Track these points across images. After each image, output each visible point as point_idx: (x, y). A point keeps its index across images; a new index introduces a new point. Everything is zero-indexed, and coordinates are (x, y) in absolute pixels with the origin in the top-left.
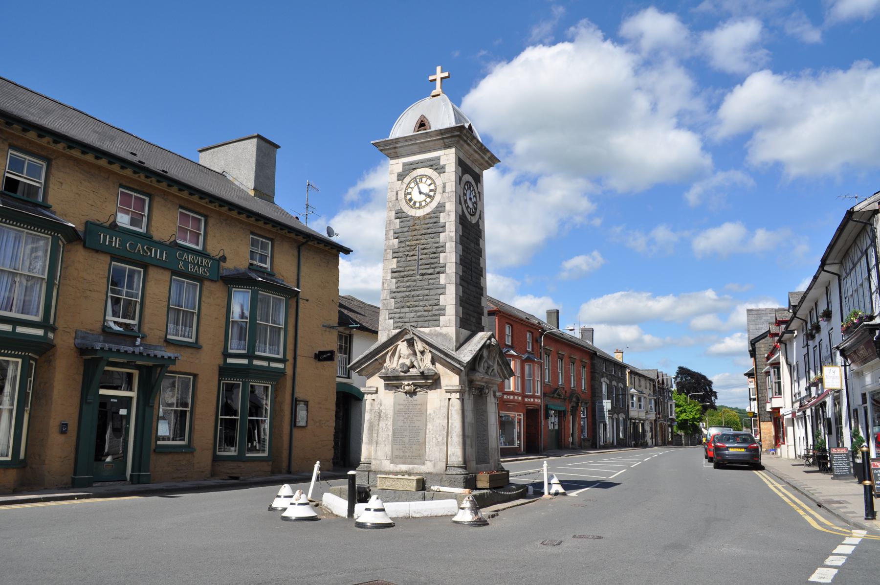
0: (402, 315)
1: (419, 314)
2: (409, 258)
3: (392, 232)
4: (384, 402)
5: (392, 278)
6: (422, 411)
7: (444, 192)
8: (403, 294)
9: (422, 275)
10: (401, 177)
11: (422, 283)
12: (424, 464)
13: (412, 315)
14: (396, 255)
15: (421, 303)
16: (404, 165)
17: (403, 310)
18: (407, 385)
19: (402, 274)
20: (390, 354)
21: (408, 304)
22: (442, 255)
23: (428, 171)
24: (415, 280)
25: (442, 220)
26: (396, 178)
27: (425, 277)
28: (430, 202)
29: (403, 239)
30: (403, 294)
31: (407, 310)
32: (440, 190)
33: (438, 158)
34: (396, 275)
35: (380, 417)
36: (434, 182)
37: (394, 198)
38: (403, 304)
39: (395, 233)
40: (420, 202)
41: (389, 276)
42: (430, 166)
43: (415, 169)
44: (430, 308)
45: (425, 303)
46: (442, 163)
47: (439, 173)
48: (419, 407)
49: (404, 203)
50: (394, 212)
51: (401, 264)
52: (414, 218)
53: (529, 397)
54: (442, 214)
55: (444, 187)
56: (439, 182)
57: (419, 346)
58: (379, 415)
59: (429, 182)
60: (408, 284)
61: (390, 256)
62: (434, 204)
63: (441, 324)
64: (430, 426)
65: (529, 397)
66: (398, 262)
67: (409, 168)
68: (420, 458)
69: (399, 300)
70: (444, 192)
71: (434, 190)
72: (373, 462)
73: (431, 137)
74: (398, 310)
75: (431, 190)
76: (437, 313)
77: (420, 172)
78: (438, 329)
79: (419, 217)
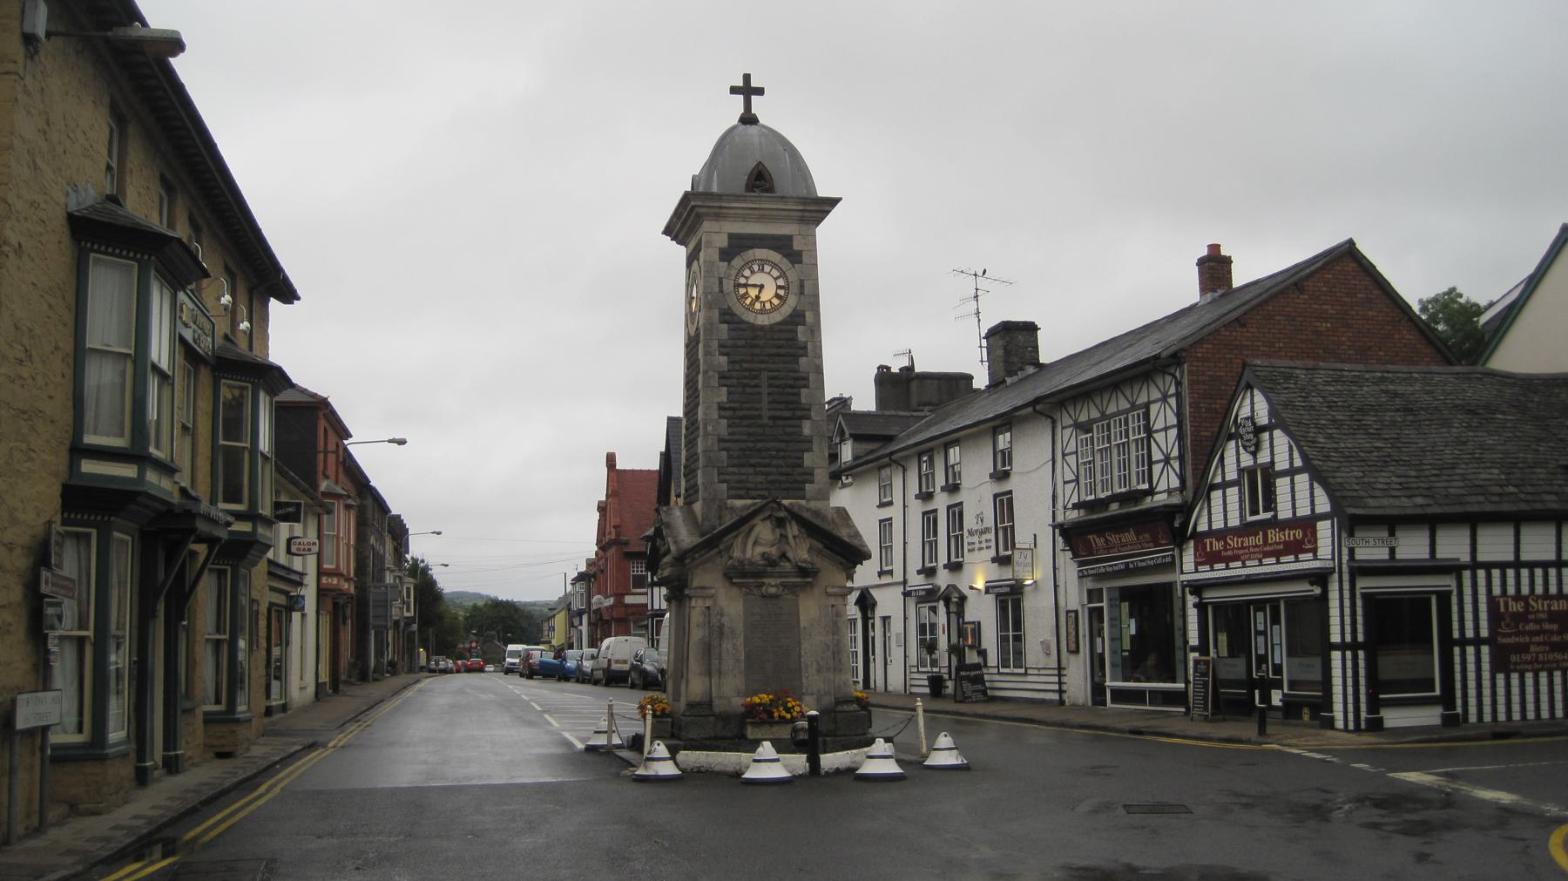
2: (749, 390)
3: (715, 344)
5: (721, 417)
7: (802, 293)
8: (743, 445)
10: (727, 255)
13: (760, 478)
16: (731, 236)
17: (743, 470)
18: (772, 585)
19: (740, 413)
21: (752, 461)
22: (804, 391)
23: (775, 256)
26: (716, 257)
27: (779, 422)
28: (780, 306)
29: (738, 358)
31: (751, 470)
32: (794, 288)
33: (789, 238)
34: (728, 413)
35: (721, 634)
37: (716, 289)
39: (721, 346)
42: (776, 249)
43: (751, 248)
44: (789, 470)
46: (796, 247)
47: (793, 263)
50: (717, 312)
52: (753, 327)
53: (330, 574)
54: (800, 328)
55: (802, 286)
58: (720, 631)
59: (775, 273)
60: (751, 430)
61: (715, 382)
62: (786, 310)
63: (808, 495)
64: (805, 645)
65: (330, 574)
66: (729, 393)
67: (737, 246)
69: (736, 454)
70: (802, 293)
72: (716, 702)
77: (761, 253)
78: (803, 502)
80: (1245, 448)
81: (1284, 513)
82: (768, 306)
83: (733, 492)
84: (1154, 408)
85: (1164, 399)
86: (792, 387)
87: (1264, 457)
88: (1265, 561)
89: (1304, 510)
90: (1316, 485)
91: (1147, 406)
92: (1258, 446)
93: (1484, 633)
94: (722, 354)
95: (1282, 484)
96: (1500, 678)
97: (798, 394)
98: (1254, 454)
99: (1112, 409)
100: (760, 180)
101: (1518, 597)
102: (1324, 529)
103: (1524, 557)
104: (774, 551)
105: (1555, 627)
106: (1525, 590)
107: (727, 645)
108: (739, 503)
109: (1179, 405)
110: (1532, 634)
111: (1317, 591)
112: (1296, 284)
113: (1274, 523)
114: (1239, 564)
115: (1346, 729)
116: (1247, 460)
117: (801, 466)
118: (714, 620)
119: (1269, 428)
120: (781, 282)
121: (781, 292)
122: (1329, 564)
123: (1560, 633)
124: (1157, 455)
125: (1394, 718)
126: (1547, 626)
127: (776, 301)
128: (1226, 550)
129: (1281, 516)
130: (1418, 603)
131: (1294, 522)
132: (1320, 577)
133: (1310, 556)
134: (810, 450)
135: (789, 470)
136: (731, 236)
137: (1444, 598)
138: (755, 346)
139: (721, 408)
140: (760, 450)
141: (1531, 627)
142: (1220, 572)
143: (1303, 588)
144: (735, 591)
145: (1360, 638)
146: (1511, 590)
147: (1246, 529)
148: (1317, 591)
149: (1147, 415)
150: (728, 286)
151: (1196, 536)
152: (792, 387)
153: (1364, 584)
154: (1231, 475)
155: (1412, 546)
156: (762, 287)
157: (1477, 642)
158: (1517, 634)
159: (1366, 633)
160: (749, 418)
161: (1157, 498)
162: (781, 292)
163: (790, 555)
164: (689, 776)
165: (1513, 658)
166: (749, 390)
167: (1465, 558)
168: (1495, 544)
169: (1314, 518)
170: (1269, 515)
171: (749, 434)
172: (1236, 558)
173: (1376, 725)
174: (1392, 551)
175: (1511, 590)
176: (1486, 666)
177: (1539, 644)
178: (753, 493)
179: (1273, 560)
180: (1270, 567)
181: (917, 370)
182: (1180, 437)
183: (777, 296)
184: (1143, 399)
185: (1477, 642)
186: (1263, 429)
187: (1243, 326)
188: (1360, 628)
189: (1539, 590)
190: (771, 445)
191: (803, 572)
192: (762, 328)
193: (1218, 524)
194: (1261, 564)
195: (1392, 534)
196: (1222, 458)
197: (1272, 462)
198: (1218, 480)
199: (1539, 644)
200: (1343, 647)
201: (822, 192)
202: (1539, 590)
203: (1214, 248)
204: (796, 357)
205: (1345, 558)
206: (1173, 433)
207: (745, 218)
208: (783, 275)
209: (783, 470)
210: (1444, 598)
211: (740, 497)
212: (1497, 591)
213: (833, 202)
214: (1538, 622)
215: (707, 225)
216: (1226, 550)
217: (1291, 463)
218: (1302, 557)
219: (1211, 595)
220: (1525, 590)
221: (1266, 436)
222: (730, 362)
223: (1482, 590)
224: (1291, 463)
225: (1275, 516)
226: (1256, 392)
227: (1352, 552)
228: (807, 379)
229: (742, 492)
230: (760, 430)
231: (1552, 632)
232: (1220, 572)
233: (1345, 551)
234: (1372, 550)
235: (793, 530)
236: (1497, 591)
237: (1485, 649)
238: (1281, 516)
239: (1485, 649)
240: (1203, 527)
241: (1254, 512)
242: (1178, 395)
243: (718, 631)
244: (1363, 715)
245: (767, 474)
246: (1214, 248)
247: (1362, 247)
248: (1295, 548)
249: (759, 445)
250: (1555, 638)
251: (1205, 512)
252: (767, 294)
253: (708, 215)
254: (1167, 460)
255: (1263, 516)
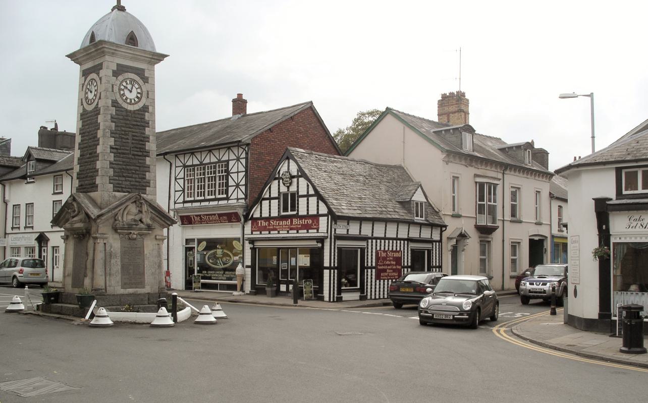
0: (121, 182)
1: (132, 183)
2: (124, 141)
3: (109, 117)
4: (113, 245)
6: (141, 252)
7: (148, 97)
8: (120, 167)
9: (133, 155)
10: (116, 74)
11: (134, 161)
12: (144, 287)
13: (128, 183)
14: (113, 135)
15: (134, 176)
16: (118, 65)
17: (120, 178)
18: (134, 233)
19: (119, 151)
20: (122, 210)
24: (129, 158)
25: (147, 118)
27: (137, 157)
28: (139, 102)
30: (120, 167)
31: (124, 179)
32: (145, 94)
33: (143, 70)
34: (115, 151)
35: (111, 255)
36: (140, 87)
38: (121, 174)
39: (112, 118)
40: (131, 100)
41: (108, 150)
42: (138, 74)
45: (137, 176)
46: (146, 75)
48: (139, 249)
49: (119, 96)
51: (118, 143)
52: (126, 110)
54: (146, 113)
55: (148, 94)
56: (144, 89)
57: (145, 208)
60: (124, 160)
61: (109, 134)
62: (141, 105)
64: (146, 262)
66: (115, 141)
68: (141, 284)
70: (148, 97)
71: (141, 94)
73: (145, 53)
74: (117, 178)
75: (123, 90)
76: (144, 184)
79: (131, 110)
80: (284, 184)
81: (302, 211)
82: (133, 101)
83: (115, 189)
84: (231, 163)
85: (238, 159)
86: (142, 141)
87: (293, 189)
88: (290, 232)
89: (313, 212)
90: (320, 202)
91: (228, 161)
92: (291, 184)
93: (374, 265)
94: (112, 122)
95: (302, 202)
96: (378, 281)
97: (145, 145)
98: (288, 187)
99: (207, 161)
100: (132, 39)
101: (384, 251)
102: (323, 221)
103: (387, 236)
104: (137, 218)
105: (394, 263)
106: (387, 249)
107: (113, 261)
108: (118, 194)
109: (247, 163)
110: (388, 265)
111: (320, 245)
112: (291, 117)
113: (297, 216)
114: (276, 232)
115: (329, 301)
116: (284, 189)
117: (145, 178)
118: (108, 249)
119: (298, 177)
120: (139, 91)
121: (139, 95)
122: (326, 235)
123: (396, 265)
124: (231, 183)
125: (345, 296)
126: (392, 263)
127: (137, 100)
128: (269, 226)
129: (300, 214)
130: (353, 251)
131: (308, 216)
132: (321, 240)
133: (315, 231)
134: (149, 172)
135: (140, 180)
136: (118, 65)
137: (363, 250)
138: (128, 120)
139: (111, 148)
140: (128, 170)
141: (388, 262)
142: (265, 234)
143: (313, 244)
144: (117, 236)
145: (336, 265)
146: (382, 249)
147: (281, 218)
148: (320, 245)
149: (227, 166)
150: (116, 89)
151: (253, 219)
152: (142, 141)
153: (340, 243)
154: (274, 194)
155: (354, 230)
156: (131, 92)
157: (371, 268)
158: (384, 265)
159: (411, 262)
160: (124, 154)
161: (230, 202)
162: (139, 95)
163: (144, 220)
164: (117, 324)
165: (382, 274)
166: (124, 141)
167: (370, 235)
168: (379, 230)
169: (317, 217)
170: (295, 213)
171: (123, 162)
172: (275, 230)
173: (339, 300)
174: (348, 230)
175: (382, 249)
176: (374, 277)
177: (389, 269)
178: (124, 190)
179: (295, 231)
180: (293, 234)
181: (60, 130)
182: (246, 176)
183: (137, 97)
184: (225, 158)
185: (371, 268)
186: (294, 177)
187: (271, 132)
188: (409, 261)
189: (391, 249)
190: (132, 168)
191: (149, 228)
192: (130, 111)
193: (265, 214)
194: (288, 233)
195: (348, 224)
196: (270, 187)
197: (298, 193)
198: (267, 196)
199: (389, 269)
200: (330, 268)
201: (159, 50)
202: (391, 249)
203: (240, 95)
204: (144, 127)
205: (333, 233)
206: (242, 175)
207: (125, 58)
208: (140, 87)
209: (138, 180)
210: (363, 250)
211: (119, 191)
212: (378, 249)
213: (166, 56)
214: (390, 261)
215: (107, 58)
216: (269, 226)
217: (308, 192)
218: (310, 231)
219: (258, 244)
220: (387, 249)
221: (295, 180)
222: (116, 126)
223: (374, 248)
224: (308, 192)
225: (298, 213)
226: (291, 161)
227: (335, 230)
228: (148, 138)
229: (120, 189)
230: (128, 160)
231: (393, 265)
232: (265, 234)
233: (333, 230)
234: (341, 231)
235: (145, 208)
236: (378, 249)
237: (374, 270)
238: (300, 214)
239: (374, 270)
240: (257, 215)
241: (285, 209)
242: (246, 158)
243: (108, 256)
244: (336, 295)
245: (130, 181)
246: (240, 95)
247: (316, 105)
248: (307, 227)
249: (128, 167)
250: (394, 267)
251: (259, 209)
252: (132, 96)
253: (109, 52)
254: (237, 186)
255: (290, 213)
